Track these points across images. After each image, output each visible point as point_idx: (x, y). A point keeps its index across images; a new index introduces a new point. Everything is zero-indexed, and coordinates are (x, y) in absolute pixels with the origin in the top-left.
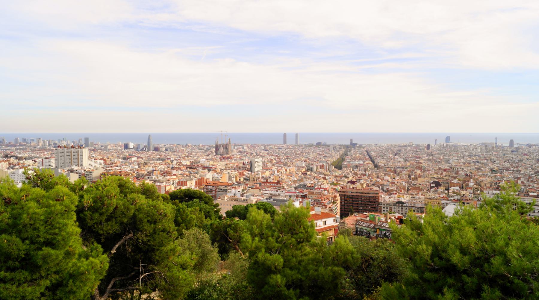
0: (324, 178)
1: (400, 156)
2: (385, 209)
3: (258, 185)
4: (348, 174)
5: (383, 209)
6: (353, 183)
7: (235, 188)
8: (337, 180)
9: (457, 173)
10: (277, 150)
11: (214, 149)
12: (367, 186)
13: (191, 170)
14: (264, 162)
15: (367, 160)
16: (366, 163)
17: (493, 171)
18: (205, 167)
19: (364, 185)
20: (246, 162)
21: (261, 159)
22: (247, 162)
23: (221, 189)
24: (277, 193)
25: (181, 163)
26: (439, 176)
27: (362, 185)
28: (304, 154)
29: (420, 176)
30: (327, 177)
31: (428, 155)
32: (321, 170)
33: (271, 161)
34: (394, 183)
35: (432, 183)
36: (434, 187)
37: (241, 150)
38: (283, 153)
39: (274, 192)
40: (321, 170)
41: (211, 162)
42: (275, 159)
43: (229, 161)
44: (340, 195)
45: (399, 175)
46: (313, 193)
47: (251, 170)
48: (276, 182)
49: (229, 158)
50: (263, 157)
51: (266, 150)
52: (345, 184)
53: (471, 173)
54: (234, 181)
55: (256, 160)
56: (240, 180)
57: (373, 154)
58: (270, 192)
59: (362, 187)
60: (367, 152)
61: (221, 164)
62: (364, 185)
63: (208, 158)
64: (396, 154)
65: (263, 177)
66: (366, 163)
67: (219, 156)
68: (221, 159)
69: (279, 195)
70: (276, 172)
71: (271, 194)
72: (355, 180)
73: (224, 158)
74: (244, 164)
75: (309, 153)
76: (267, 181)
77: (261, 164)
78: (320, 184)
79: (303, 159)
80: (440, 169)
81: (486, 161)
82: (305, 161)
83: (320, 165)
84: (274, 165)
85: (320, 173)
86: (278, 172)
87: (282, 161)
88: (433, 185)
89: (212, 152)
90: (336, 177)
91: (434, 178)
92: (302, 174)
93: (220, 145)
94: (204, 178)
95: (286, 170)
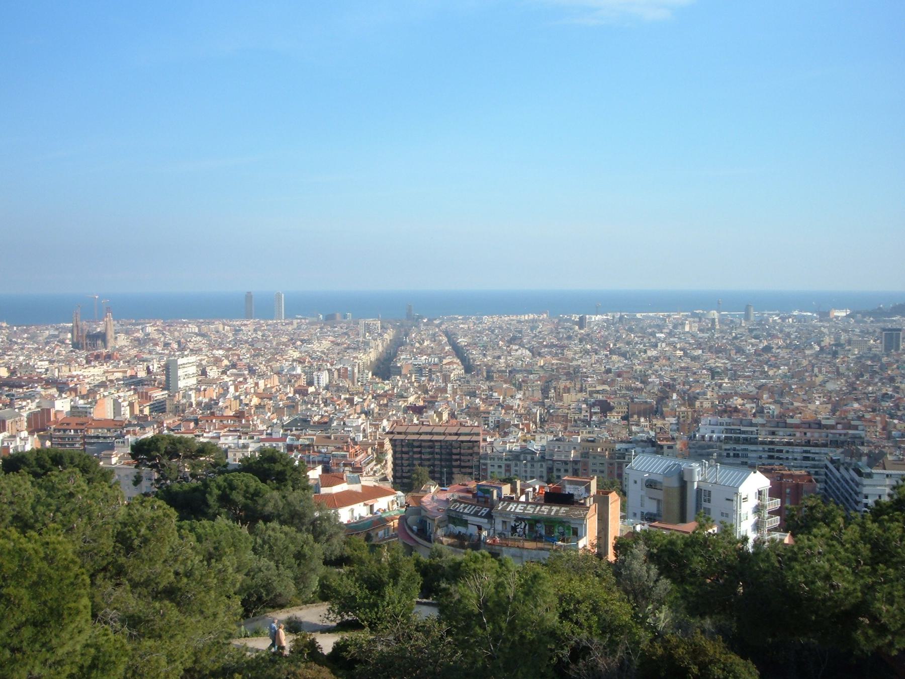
0: (350, 401)
1: (522, 345)
2: (496, 470)
3: (192, 425)
4: (407, 389)
5: (490, 469)
6: (418, 410)
8: (380, 405)
9: (645, 382)
12: (452, 415)
14: (199, 365)
15: (447, 354)
16: (445, 361)
17: (713, 373)
19: (445, 416)
20: (155, 367)
21: (193, 359)
26: (606, 387)
27: (440, 415)
28: (299, 343)
29: (567, 390)
30: (356, 399)
31: (581, 341)
33: (217, 361)
34: (511, 408)
35: (594, 405)
36: (595, 413)
37: (140, 335)
38: (246, 342)
42: (227, 357)
44: (391, 440)
45: (519, 388)
48: (232, 414)
49: (109, 357)
50: (194, 352)
51: (203, 335)
52: (400, 414)
53: (674, 380)
54: (128, 416)
55: (180, 361)
56: (141, 411)
57: (462, 341)
59: (441, 419)
60: (447, 334)
61: (95, 373)
62: (445, 416)
64: (512, 341)
65: (199, 404)
66: (445, 361)
70: (232, 389)
72: (421, 403)
73: (97, 357)
75: (309, 341)
77: (193, 370)
79: (296, 355)
80: (608, 371)
81: (700, 352)
82: (301, 361)
83: (339, 370)
84: (224, 373)
85: (339, 389)
86: (236, 390)
87: (245, 361)
88: (596, 409)
91: (598, 392)
92: (296, 392)
94: (48, 411)
95: (257, 384)
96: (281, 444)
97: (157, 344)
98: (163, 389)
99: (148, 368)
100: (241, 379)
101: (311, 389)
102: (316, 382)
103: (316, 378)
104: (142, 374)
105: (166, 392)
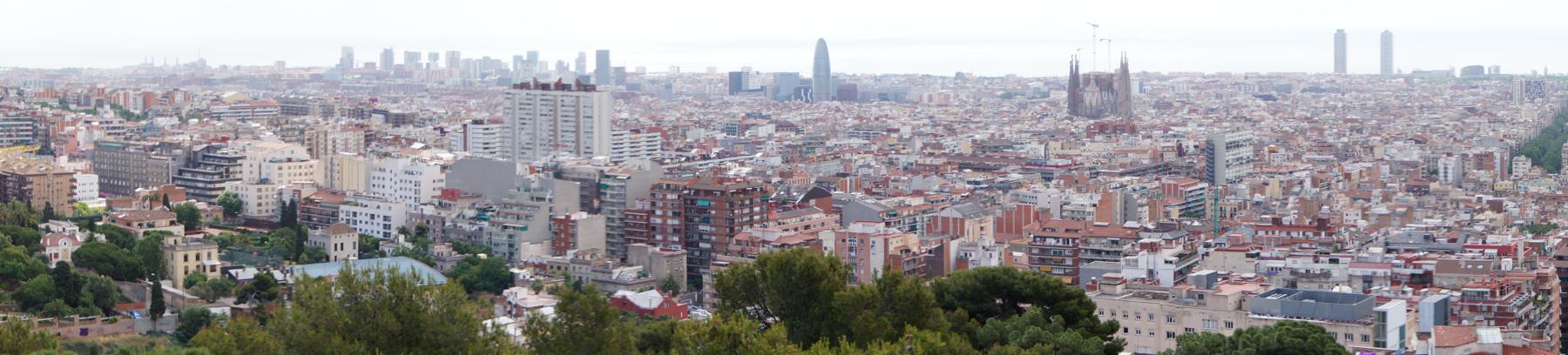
0: (1497, 207)
7: (1153, 248)
10: (1308, 95)
11: (1065, 94)
13: (980, 177)
18: (1029, 165)
20: (1189, 145)
22: (1191, 144)
23: (1099, 252)
24: (1317, 268)
25: (940, 146)
32: (1483, 175)
38: (1334, 108)
39: (1302, 264)
40: (1483, 175)
41: (1055, 147)
43: (1124, 140)
46: (1453, 267)
47: (1209, 175)
51: (1266, 98)
58: (1289, 262)
63: (1040, 127)
67: (1082, 124)
68: (1090, 133)
69: (1326, 275)
71: (1294, 272)
73: (1102, 129)
74: (1181, 152)
76: (1277, 222)
78: (1479, 228)
84: (1298, 157)
86: (1315, 183)
89: (1055, 104)
90: (1540, 199)
93: (1087, 78)
96: (1380, 272)
97: (1195, 111)
98: (1202, 180)
99: (1180, 147)
100: (1323, 167)
101: (1433, 186)
102: (1441, 174)
103: (1441, 166)
104: (1170, 157)
105: (1205, 185)
